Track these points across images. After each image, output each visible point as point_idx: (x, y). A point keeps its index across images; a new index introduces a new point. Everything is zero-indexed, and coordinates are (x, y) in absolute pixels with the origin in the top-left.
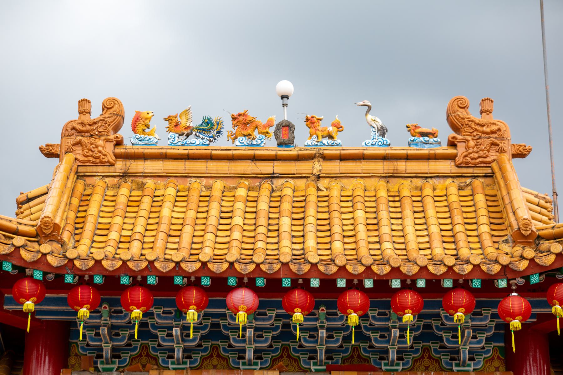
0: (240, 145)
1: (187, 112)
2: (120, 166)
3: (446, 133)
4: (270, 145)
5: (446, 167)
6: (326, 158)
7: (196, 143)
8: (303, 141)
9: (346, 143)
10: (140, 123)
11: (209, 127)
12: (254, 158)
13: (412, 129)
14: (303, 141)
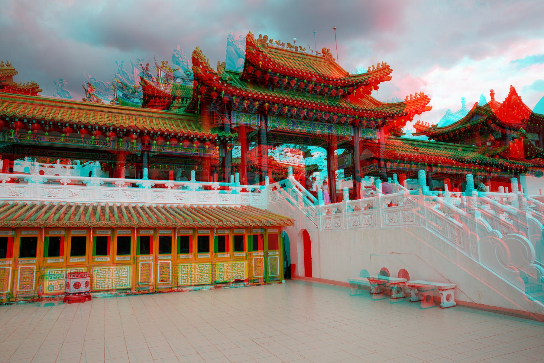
1: (279, 41)
2: (269, 49)
3: (322, 54)
4: (294, 50)
5: (323, 60)
7: (281, 47)
8: (299, 50)
9: (306, 52)
10: (271, 41)
11: (283, 44)
13: (317, 52)
14: (299, 50)
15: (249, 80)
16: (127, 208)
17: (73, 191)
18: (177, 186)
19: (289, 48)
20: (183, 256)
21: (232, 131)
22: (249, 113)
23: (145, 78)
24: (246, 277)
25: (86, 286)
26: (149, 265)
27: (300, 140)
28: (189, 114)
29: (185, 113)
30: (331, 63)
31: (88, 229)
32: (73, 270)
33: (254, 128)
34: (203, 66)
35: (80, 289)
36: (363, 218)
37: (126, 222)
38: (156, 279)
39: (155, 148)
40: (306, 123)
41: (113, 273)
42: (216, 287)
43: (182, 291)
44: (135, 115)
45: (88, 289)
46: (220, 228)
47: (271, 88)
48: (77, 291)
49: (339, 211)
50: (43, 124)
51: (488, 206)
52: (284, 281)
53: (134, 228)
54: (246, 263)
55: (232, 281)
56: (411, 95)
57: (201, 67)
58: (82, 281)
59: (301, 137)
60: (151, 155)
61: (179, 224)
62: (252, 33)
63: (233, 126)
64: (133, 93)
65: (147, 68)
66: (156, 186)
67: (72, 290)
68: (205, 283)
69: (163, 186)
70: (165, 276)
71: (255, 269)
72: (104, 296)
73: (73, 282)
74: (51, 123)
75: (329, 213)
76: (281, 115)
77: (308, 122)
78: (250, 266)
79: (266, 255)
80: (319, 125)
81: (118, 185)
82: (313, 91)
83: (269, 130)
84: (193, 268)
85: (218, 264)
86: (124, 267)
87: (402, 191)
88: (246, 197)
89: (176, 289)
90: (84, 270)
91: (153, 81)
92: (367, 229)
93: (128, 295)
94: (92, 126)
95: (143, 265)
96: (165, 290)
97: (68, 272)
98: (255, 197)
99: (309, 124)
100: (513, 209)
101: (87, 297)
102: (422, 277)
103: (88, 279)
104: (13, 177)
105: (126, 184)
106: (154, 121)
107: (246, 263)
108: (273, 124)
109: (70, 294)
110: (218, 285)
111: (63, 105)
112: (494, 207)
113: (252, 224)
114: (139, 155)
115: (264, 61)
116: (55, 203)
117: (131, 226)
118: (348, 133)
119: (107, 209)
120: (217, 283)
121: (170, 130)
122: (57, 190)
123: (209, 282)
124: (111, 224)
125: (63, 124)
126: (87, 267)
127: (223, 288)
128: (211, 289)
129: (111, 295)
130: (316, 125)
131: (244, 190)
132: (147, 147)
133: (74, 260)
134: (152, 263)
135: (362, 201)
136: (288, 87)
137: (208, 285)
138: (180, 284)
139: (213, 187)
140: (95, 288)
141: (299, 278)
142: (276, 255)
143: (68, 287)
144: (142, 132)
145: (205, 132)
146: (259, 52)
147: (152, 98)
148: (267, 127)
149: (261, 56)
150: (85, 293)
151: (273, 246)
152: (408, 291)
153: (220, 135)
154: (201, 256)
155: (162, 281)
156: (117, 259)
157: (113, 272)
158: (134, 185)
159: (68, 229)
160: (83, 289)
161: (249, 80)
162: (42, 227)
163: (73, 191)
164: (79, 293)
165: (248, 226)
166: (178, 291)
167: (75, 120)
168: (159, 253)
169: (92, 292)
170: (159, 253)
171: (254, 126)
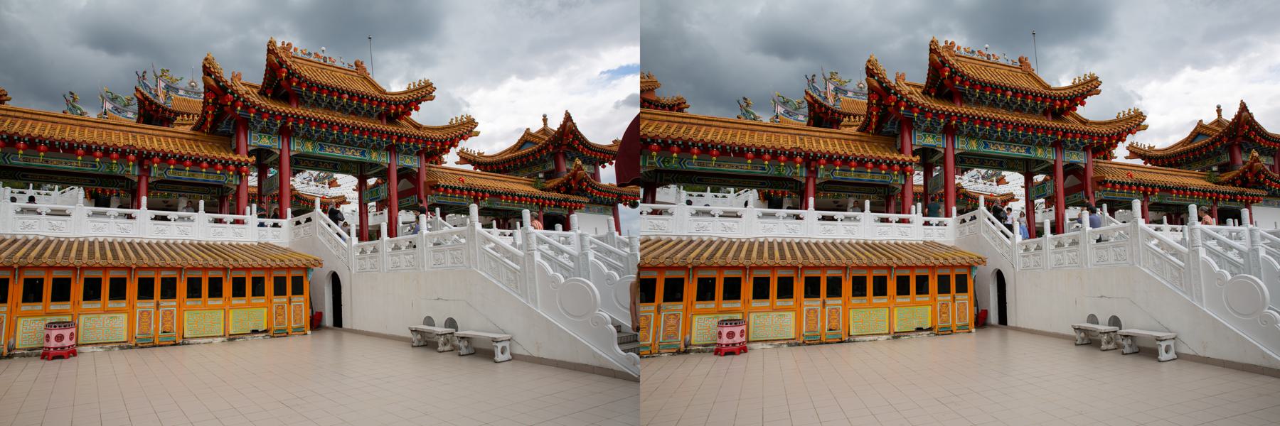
16: (121, 244)
18: (181, 218)
21: (250, 154)
36: (404, 258)
37: (122, 260)
39: (156, 172)
46: (235, 269)
49: (375, 250)
51: (546, 246)
54: (265, 310)
61: (185, 264)
62: (274, 39)
66: (157, 218)
70: (167, 328)
75: (363, 252)
79: (290, 301)
84: (201, 317)
87: (448, 227)
100: (573, 249)
102: (471, 327)
106: (155, 140)
107: (265, 310)
112: (552, 247)
113: (274, 265)
115: (288, 73)
116: (31, 237)
119: (86, 245)
124: (103, 263)
125: (42, 140)
132: (146, 172)
135: (403, 239)
140: (80, 342)
141: (327, 328)
142: (299, 300)
144: (140, 152)
146: (282, 62)
147: (153, 113)
151: (298, 290)
152: (457, 343)
153: (235, 158)
158: (129, 217)
167: (57, 135)
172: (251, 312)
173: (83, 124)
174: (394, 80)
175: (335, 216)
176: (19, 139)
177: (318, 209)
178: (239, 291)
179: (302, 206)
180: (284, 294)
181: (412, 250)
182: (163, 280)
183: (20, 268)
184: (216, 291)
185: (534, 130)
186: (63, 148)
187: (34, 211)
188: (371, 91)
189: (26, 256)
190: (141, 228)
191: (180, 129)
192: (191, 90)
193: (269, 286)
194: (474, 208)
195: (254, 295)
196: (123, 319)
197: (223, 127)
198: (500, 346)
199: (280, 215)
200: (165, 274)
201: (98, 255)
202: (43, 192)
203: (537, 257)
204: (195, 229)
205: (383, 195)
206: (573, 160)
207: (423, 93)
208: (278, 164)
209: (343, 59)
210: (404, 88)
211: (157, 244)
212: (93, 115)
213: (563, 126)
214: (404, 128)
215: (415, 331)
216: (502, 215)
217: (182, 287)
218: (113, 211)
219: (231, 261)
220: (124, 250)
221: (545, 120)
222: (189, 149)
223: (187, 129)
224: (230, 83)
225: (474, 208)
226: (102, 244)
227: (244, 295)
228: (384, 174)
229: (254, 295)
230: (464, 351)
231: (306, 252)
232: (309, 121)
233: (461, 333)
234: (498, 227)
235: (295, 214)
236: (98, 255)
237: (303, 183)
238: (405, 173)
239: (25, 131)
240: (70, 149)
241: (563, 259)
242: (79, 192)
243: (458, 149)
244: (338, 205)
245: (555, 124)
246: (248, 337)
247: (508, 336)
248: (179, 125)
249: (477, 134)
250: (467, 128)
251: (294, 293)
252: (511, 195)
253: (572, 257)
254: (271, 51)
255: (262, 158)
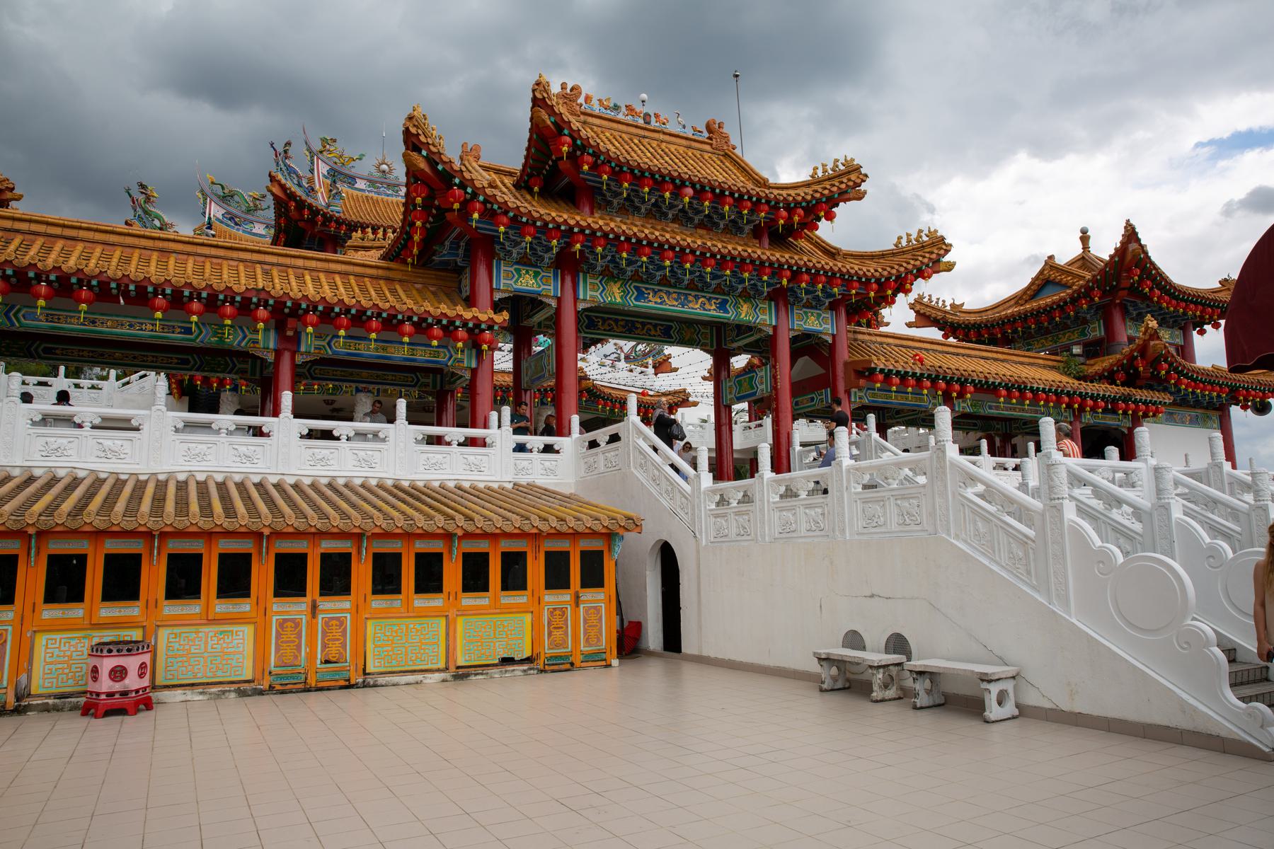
0: (629, 119)
2: (582, 118)
3: (706, 134)
4: (641, 122)
5: (707, 148)
6: (664, 133)
7: (611, 114)
8: (654, 124)
9: (671, 128)
11: (616, 108)
12: (636, 127)
14: (654, 124)
15: (536, 189)
16: (241, 486)
17: (108, 443)
18: (361, 435)
19: (629, 118)
20: (379, 602)
21: (497, 307)
22: (536, 266)
23: (280, 177)
24: (527, 654)
25: (141, 676)
26: (297, 624)
27: (653, 332)
28: (392, 265)
29: (383, 263)
30: (726, 155)
31: (149, 535)
32: (108, 636)
33: (544, 300)
34: (429, 151)
35: (127, 681)
36: (804, 514)
37: (243, 518)
38: (311, 656)
39: (310, 343)
40: (668, 294)
41: (206, 643)
42: (457, 677)
43: (375, 686)
44: (260, 263)
45: (146, 682)
46: (468, 535)
47: (587, 209)
48: (117, 687)
49: (747, 499)
50: (31, 279)
51: (1088, 490)
52: (615, 662)
53: (260, 535)
55: (496, 661)
56: (908, 235)
57: (424, 153)
58: (132, 663)
59: (655, 326)
60: (299, 359)
61: (368, 526)
63: (497, 296)
64: (249, 211)
65: (286, 152)
66: (312, 435)
67: (106, 684)
68: (429, 666)
69: (327, 435)
70: (333, 653)
71: (550, 634)
72: (183, 698)
73: (107, 664)
74: (52, 277)
75: (723, 501)
76: (611, 274)
77: (671, 290)
78: (536, 626)
79: (577, 600)
80: (697, 298)
81: (218, 432)
82: (683, 218)
83: (581, 306)
84: (400, 631)
85: (461, 622)
86: (235, 628)
87: (893, 452)
88: (525, 463)
89: (360, 680)
90: (136, 635)
91: (300, 185)
92: (828, 539)
93: (242, 694)
94: (156, 290)
95: (282, 624)
96: (333, 684)
97: (95, 641)
98: (547, 464)
99: (675, 296)
100: (1141, 496)
101: (142, 703)
102: (938, 651)
103: (146, 658)
104: (313, 427)
105: (239, 429)
106: (308, 279)
108: (591, 293)
109: (98, 694)
110: (462, 674)
111: (82, 234)
112: (1098, 492)
113: (545, 527)
114: (271, 358)
115: (574, 145)
116: (61, 473)
117: (254, 528)
118: (762, 317)
120: (458, 668)
121: (347, 300)
122: (65, 441)
123: (442, 665)
124: (205, 524)
125: (84, 280)
126: (144, 627)
127: (473, 678)
128: (443, 681)
129: (201, 697)
130: (690, 298)
131: (520, 448)
132: (290, 342)
133: (110, 611)
134: (304, 619)
135: (802, 476)
136: (629, 207)
137: (438, 670)
138: (370, 669)
139: (529, 446)
141: (651, 654)
142: (595, 598)
143: (95, 679)
144: (280, 304)
145: (431, 309)
147: (304, 226)
148: (576, 299)
149: (566, 132)
150: (137, 691)
151: (593, 577)
153: (468, 315)
154: (422, 601)
155: (327, 662)
156: (218, 609)
157: (208, 640)
158: (258, 432)
159: (99, 535)
160: (132, 682)
161: (536, 189)
162: (31, 531)
163: (108, 443)
164: (124, 694)
165: (535, 531)
166: (365, 685)
167: (113, 269)
168: (321, 595)
169: (154, 687)
170: (321, 595)
171: (547, 296)
172: (499, 623)
173: (166, 246)
174: (784, 159)
175: (667, 430)
176: (38, 277)
177: (633, 417)
178: (475, 579)
179: (602, 410)
180: (566, 586)
181: (819, 498)
182: (325, 558)
183: (41, 534)
184: (429, 579)
185: (1062, 259)
186: (126, 294)
187: (68, 421)
188: (739, 182)
189: (51, 509)
190: (280, 455)
191: (359, 257)
192: (380, 180)
193: (536, 570)
194: (944, 416)
195: (505, 587)
196: (244, 636)
197: (444, 253)
198: (995, 689)
199: (557, 428)
200: (328, 546)
201: (194, 507)
202: (85, 382)
203: (1070, 513)
204: (389, 456)
205: (763, 388)
206: (1140, 318)
207: (843, 185)
208: (554, 326)
209: (682, 118)
210: (803, 176)
211: (313, 486)
212: (185, 229)
213: (1121, 252)
214: (804, 255)
215: (825, 660)
216: (999, 429)
217: (362, 573)
218: (225, 420)
219: (460, 520)
220: (247, 498)
221: (1085, 238)
222: (376, 297)
223: (373, 257)
224: (457, 165)
225: (944, 416)
226: (203, 487)
227: (485, 588)
228: (764, 347)
229: (505, 587)
230: (923, 700)
231: (610, 503)
232: (614, 241)
233: (917, 663)
234: (992, 452)
235: (587, 426)
236: (194, 507)
237: (603, 364)
238: (806, 345)
239: (50, 262)
240: (140, 296)
241: (1120, 516)
242: (158, 383)
243: (912, 297)
244: (672, 408)
245: (1105, 247)
246: (495, 672)
247: (1010, 670)
248: (356, 248)
249: (950, 267)
250: (929, 255)
251: (584, 585)
252: (1018, 389)
253: (1138, 513)
254: (539, 102)
255: (522, 316)
